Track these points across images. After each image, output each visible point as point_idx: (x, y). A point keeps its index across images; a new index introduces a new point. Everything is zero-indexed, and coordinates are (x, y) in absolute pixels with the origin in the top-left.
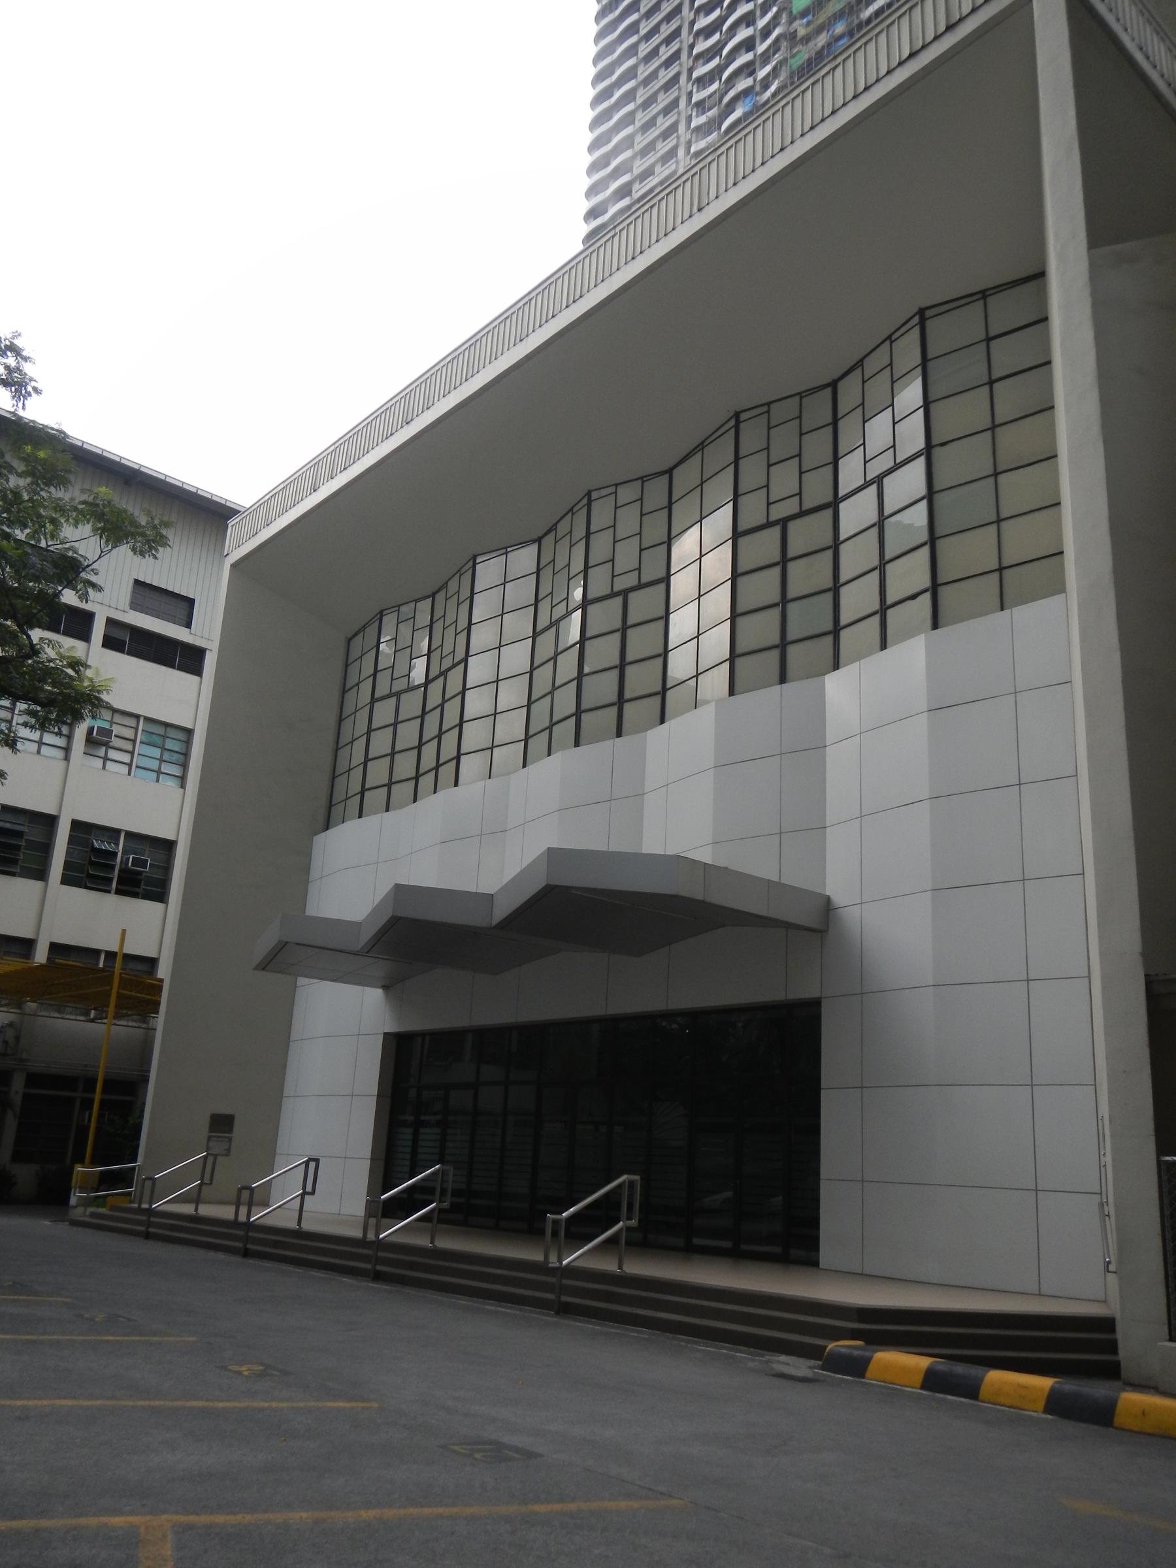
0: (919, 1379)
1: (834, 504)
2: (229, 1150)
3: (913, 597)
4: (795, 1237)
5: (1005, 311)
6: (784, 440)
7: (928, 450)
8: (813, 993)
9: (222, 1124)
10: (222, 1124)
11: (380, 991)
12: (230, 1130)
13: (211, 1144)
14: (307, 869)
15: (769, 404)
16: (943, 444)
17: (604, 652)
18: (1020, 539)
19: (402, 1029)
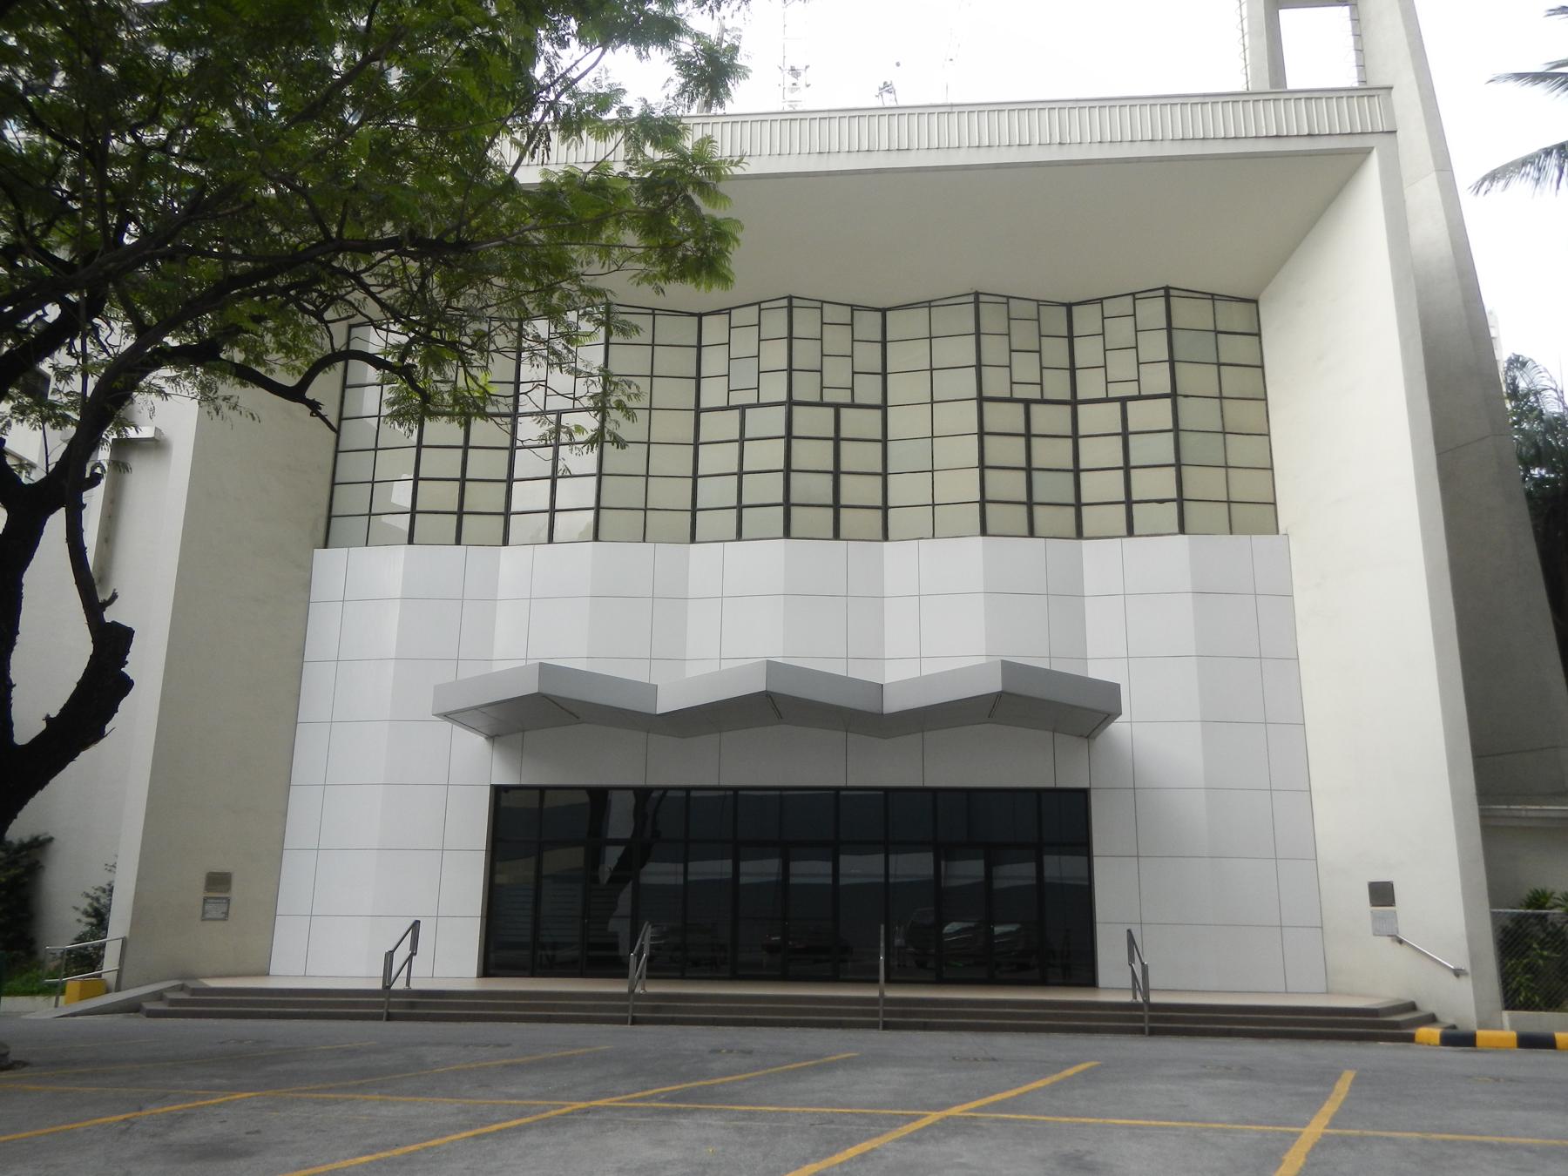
0: (1514, 1043)
1: (1074, 402)
2: (227, 913)
4: (1079, 965)
5: (1233, 316)
6: (1024, 335)
7: (1173, 395)
8: (1086, 785)
9: (218, 882)
10: (218, 882)
11: (479, 741)
12: (228, 890)
13: (208, 907)
14: (307, 586)
15: (1008, 298)
17: (814, 455)
18: (1245, 485)
19: (525, 782)
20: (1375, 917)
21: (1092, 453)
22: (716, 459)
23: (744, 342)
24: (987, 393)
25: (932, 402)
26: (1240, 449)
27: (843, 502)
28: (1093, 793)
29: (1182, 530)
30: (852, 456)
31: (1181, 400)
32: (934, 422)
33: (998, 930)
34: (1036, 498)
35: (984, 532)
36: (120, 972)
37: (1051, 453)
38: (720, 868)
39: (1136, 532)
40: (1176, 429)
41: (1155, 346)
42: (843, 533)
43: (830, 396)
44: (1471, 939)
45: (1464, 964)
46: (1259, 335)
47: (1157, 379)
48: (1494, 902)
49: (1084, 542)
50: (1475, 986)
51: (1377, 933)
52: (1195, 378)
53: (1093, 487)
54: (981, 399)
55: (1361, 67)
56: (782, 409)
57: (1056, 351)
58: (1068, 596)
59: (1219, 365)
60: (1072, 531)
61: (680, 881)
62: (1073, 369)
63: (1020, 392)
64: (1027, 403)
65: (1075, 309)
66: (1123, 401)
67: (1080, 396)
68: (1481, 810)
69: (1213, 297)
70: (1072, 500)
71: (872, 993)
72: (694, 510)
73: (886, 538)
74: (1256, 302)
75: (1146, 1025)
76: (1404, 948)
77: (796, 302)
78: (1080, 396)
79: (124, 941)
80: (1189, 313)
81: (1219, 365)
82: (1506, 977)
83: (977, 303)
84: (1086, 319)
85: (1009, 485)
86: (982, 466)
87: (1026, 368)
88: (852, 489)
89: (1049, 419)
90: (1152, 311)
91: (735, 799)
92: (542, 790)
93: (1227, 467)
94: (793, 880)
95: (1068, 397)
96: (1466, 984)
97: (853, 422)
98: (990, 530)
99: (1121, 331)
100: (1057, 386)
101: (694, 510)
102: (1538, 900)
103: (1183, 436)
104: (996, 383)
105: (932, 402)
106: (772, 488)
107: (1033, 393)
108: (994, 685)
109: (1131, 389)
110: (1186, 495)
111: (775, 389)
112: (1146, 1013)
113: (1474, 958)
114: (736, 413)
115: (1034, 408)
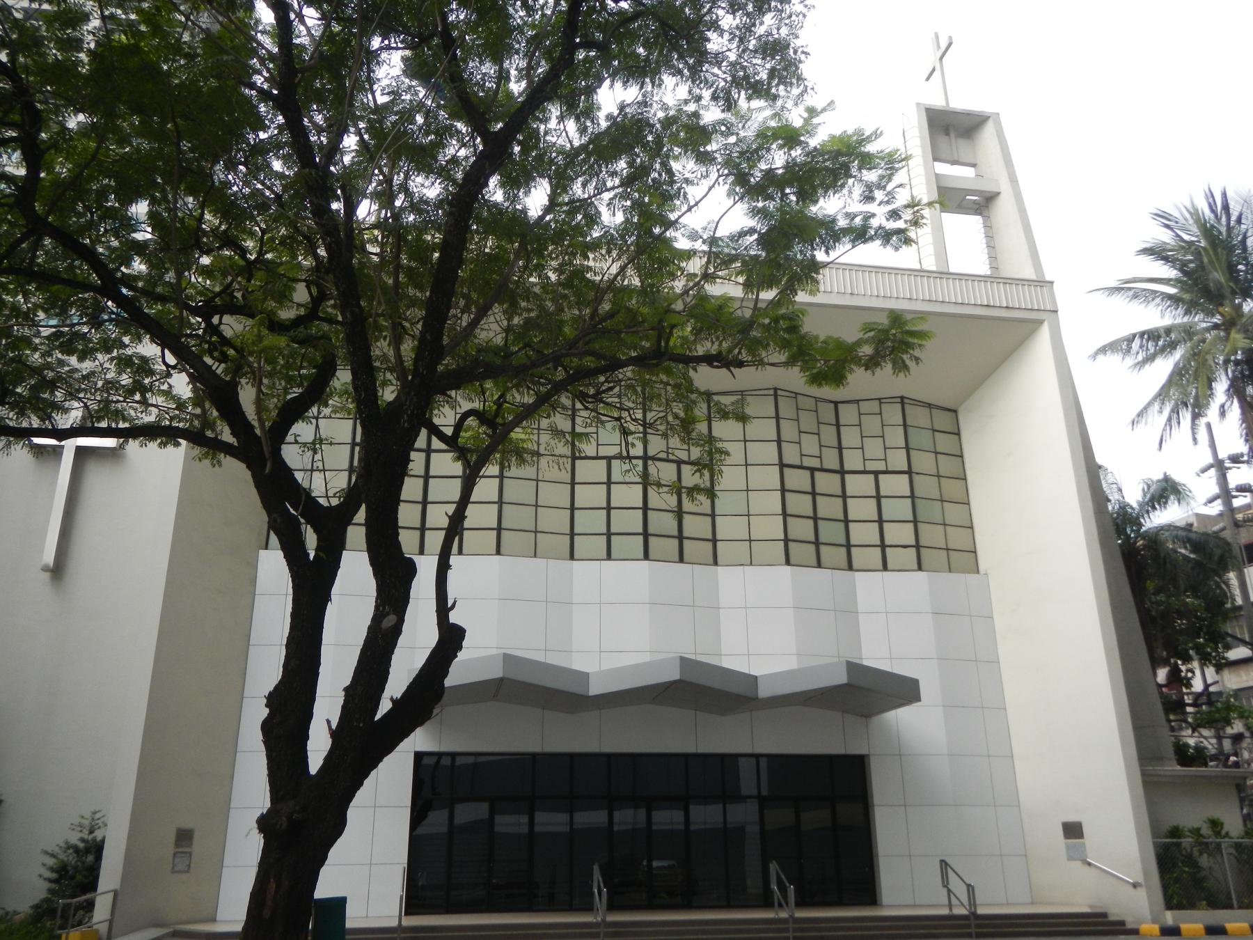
1: (842, 472)
2: (189, 866)
3: (905, 547)
5: (942, 420)
6: (808, 421)
9: (184, 837)
12: (190, 845)
13: (177, 860)
18: (957, 538)
19: (443, 749)
20: (1068, 847)
22: (590, 496)
24: (786, 461)
25: (747, 465)
26: (953, 513)
27: (686, 534)
28: (872, 758)
29: (920, 568)
31: (915, 476)
33: (655, 864)
34: (822, 539)
35: (788, 562)
36: (111, 922)
37: (830, 507)
38: (597, 817)
40: (913, 496)
42: (686, 557)
44: (1143, 861)
45: (1140, 879)
46: (958, 434)
47: (898, 460)
48: (1155, 834)
50: (1149, 897)
51: (1070, 858)
52: (924, 462)
53: (860, 534)
54: (782, 466)
55: (993, 258)
57: (829, 434)
58: (848, 612)
59: (936, 453)
60: (845, 564)
61: (567, 829)
62: (840, 448)
63: (808, 462)
64: (812, 470)
65: (840, 406)
66: (876, 473)
67: (847, 467)
68: (1142, 771)
70: (843, 542)
71: (769, 915)
72: (572, 535)
74: (955, 411)
75: (973, 930)
76: (1093, 869)
78: (847, 467)
79: (116, 893)
81: (936, 453)
82: (1165, 887)
83: (776, 395)
85: (802, 529)
86: (785, 514)
89: (827, 483)
90: (893, 413)
91: (611, 761)
92: (453, 755)
94: (654, 827)
95: (837, 467)
96: (1142, 894)
98: (792, 561)
99: (872, 425)
100: (831, 461)
101: (572, 535)
102: (1175, 832)
103: (918, 501)
104: (791, 455)
105: (747, 465)
106: (634, 521)
107: (815, 463)
108: (841, 678)
109: (880, 466)
110: (921, 543)
112: (973, 922)
113: (1146, 874)
115: (817, 474)
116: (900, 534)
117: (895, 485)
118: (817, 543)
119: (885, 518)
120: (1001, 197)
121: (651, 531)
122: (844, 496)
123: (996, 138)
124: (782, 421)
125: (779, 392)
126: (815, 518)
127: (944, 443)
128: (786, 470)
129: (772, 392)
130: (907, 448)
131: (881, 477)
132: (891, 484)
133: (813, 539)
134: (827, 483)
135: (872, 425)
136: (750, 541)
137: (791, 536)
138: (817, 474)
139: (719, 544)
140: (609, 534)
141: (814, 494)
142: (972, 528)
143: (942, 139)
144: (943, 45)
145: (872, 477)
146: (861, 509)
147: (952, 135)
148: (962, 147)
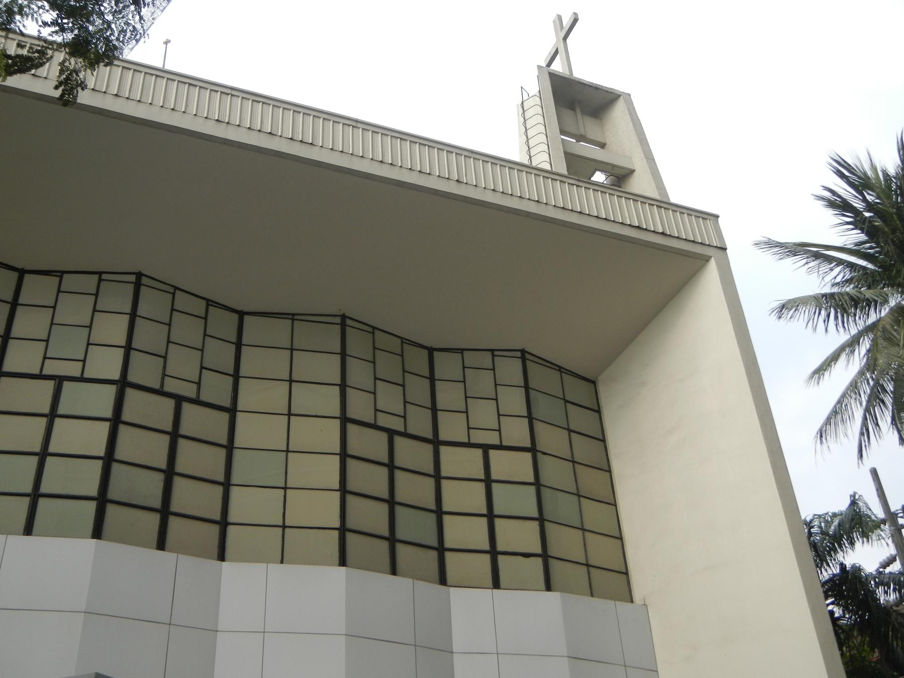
3: (527, 555)
5: (577, 391)
6: (388, 366)
16: (544, 453)
21: (456, 496)
23: (74, 309)
25: (290, 414)
27: (174, 508)
29: (549, 588)
30: (191, 457)
32: (291, 432)
35: (343, 562)
39: (502, 585)
41: (513, 401)
43: (171, 386)
49: (451, 589)
52: (551, 439)
54: (345, 420)
56: (112, 390)
57: (418, 389)
63: (384, 421)
66: (486, 448)
67: (443, 436)
69: (560, 369)
73: (222, 557)
74: (594, 383)
77: (144, 280)
80: (540, 377)
81: (570, 431)
84: (447, 366)
86: (344, 490)
87: (389, 398)
88: (186, 496)
89: (411, 454)
90: (511, 369)
93: (583, 529)
97: (194, 419)
99: (482, 382)
100: (420, 423)
104: (359, 406)
105: (290, 414)
107: (396, 424)
109: (492, 438)
111: (107, 364)
114: (50, 385)
116: (518, 535)
117: (511, 465)
118: (392, 540)
119: (497, 511)
120: (636, 174)
121: (112, 494)
122: (437, 477)
123: (628, 117)
124: (349, 360)
125: (349, 322)
126: (391, 502)
127: (580, 419)
128: (351, 427)
129: (338, 320)
130: (530, 418)
131: (493, 453)
132: (502, 464)
133: (386, 533)
134: (411, 454)
135: (482, 382)
136: (284, 527)
137: (350, 524)
138: (398, 440)
139: (231, 529)
140: (36, 495)
141: (391, 467)
142: (621, 538)
143: (568, 114)
144: (566, 22)
145: (479, 452)
146: (463, 496)
147: (578, 111)
148: (590, 127)
